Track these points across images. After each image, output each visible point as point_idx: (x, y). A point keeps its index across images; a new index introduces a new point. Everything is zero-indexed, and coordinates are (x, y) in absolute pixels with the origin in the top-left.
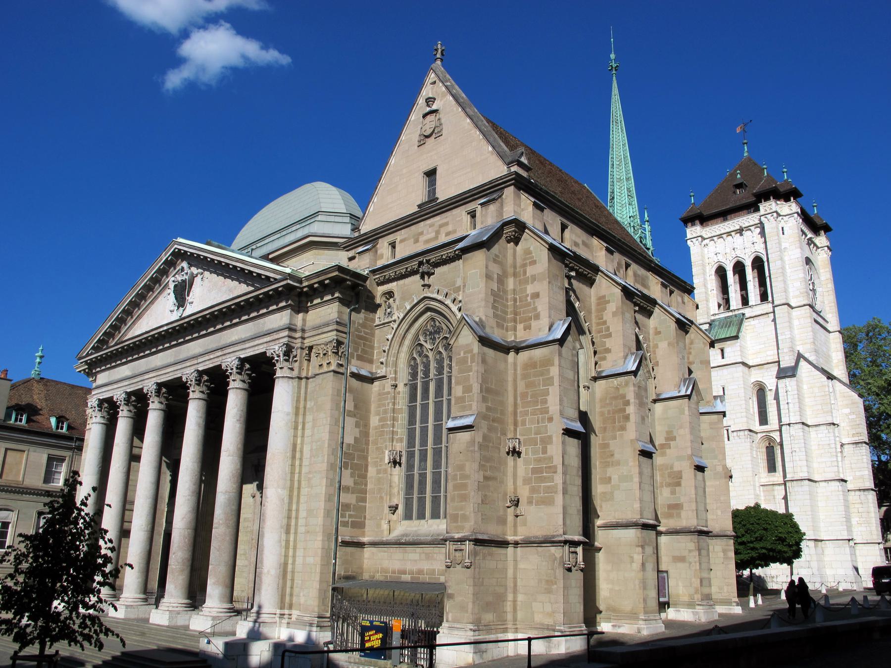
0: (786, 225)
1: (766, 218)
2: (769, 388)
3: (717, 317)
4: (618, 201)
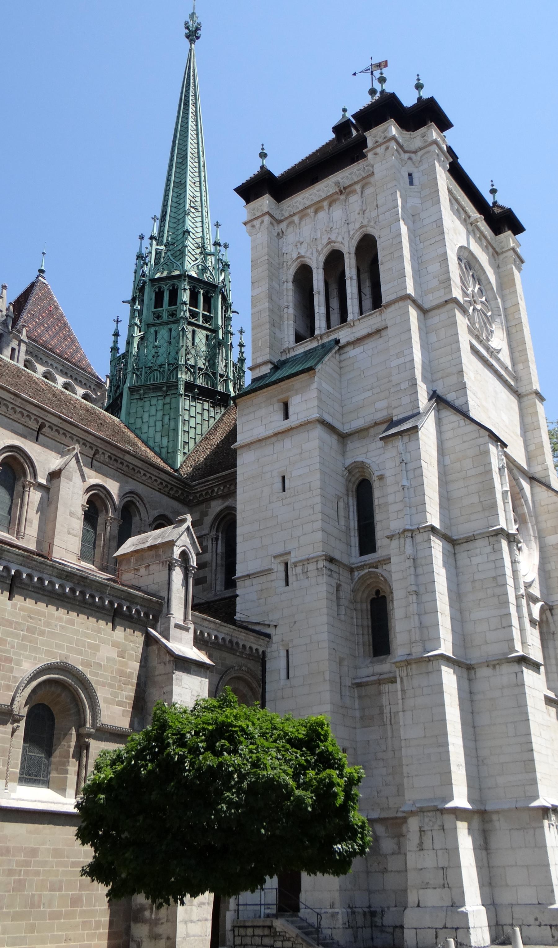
1: (376, 154)
2: (377, 474)
3: (292, 354)
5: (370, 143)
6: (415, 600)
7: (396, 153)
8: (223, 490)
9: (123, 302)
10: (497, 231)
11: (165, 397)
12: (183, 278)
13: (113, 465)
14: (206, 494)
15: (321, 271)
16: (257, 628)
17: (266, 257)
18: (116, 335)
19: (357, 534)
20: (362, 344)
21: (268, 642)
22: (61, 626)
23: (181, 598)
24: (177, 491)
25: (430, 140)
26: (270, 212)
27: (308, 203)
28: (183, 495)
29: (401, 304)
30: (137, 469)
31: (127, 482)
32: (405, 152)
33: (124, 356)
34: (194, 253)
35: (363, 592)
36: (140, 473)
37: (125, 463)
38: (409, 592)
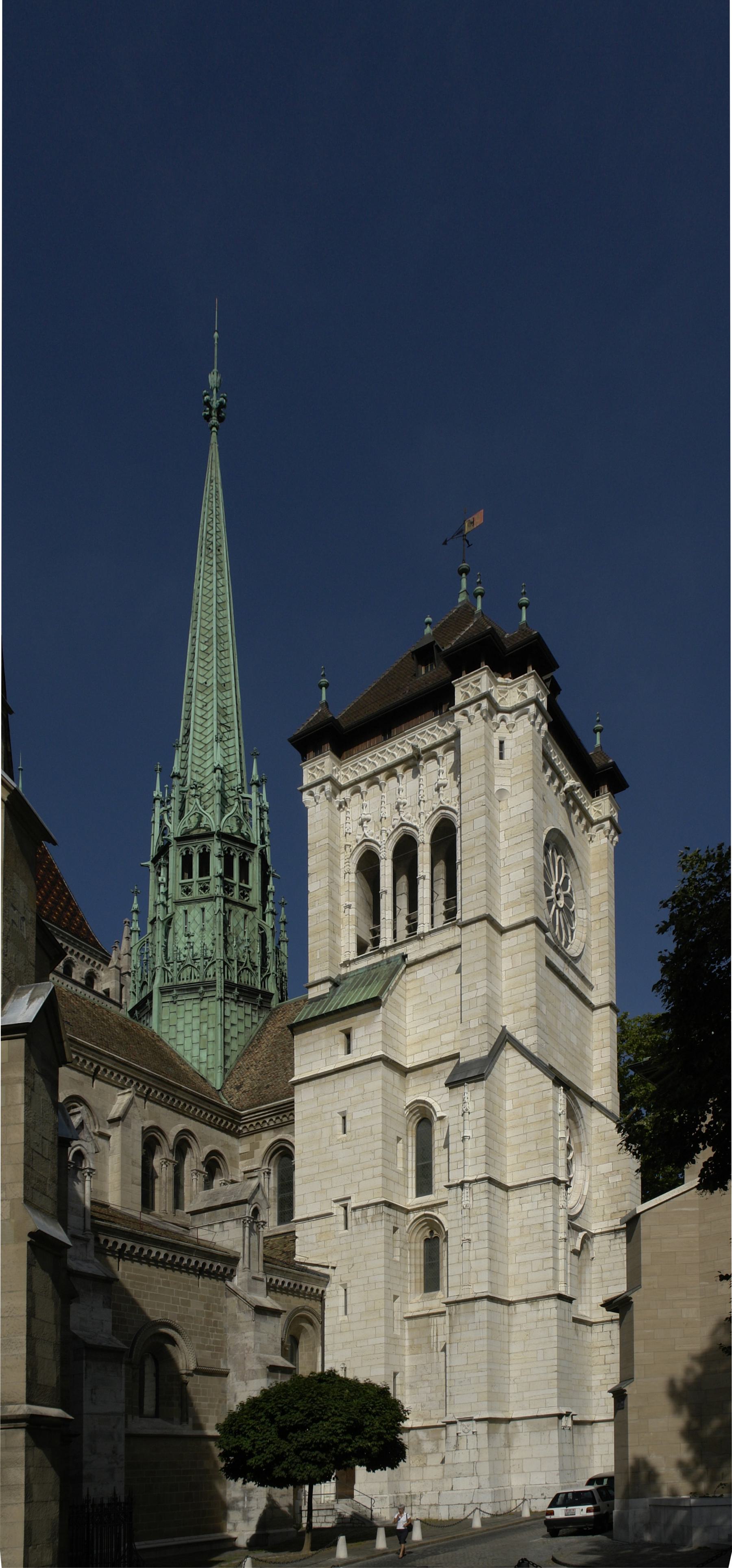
3: (354, 967)
11: (202, 1000)
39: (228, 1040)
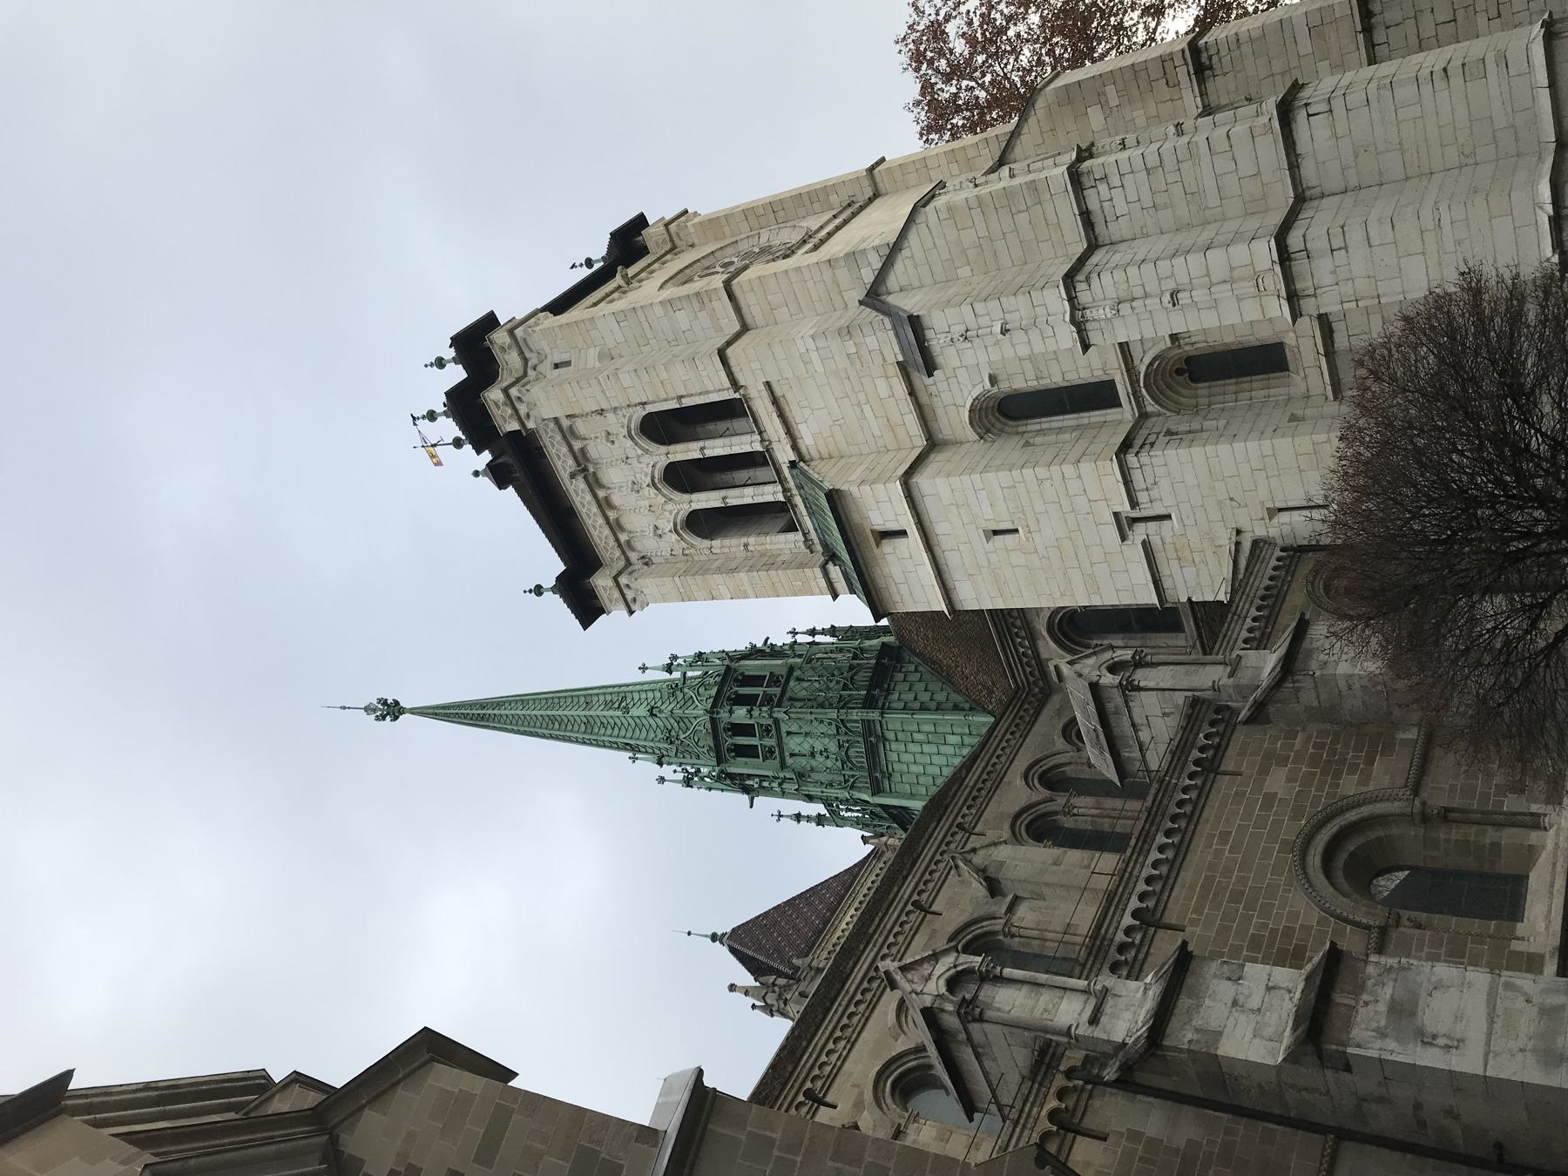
0: (549, 357)
1: (528, 416)
3: (813, 535)
4: (629, 734)
5: (515, 426)
6: (1187, 294)
7: (528, 387)
8: (1023, 638)
9: (751, 807)
10: (643, 251)
11: (886, 740)
12: (715, 716)
13: (982, 803)
14: (1028, 664)
15: (695, 496)
16: (1243, 563)
17: (677, 578)
18: (798, 817)
19: (1087, 414)
20: (795, 427)
21: (1265, 542)
22: (1229, 852)
23: (1187, 672)
24: (1025, 710)
25: (508, 340)
26: (615, 572)
27: (601, 521)
28: (1032, 702)
29: (732, 362)
30: (989, 768)
31: (1009, 783)
32: (525, 374)
33: (828, 805)
34: (682, 702)
35: (1180, 394)
36: (995, 764)
37: (980, 785)
38: (1174, 305)
39: (933, 705)
